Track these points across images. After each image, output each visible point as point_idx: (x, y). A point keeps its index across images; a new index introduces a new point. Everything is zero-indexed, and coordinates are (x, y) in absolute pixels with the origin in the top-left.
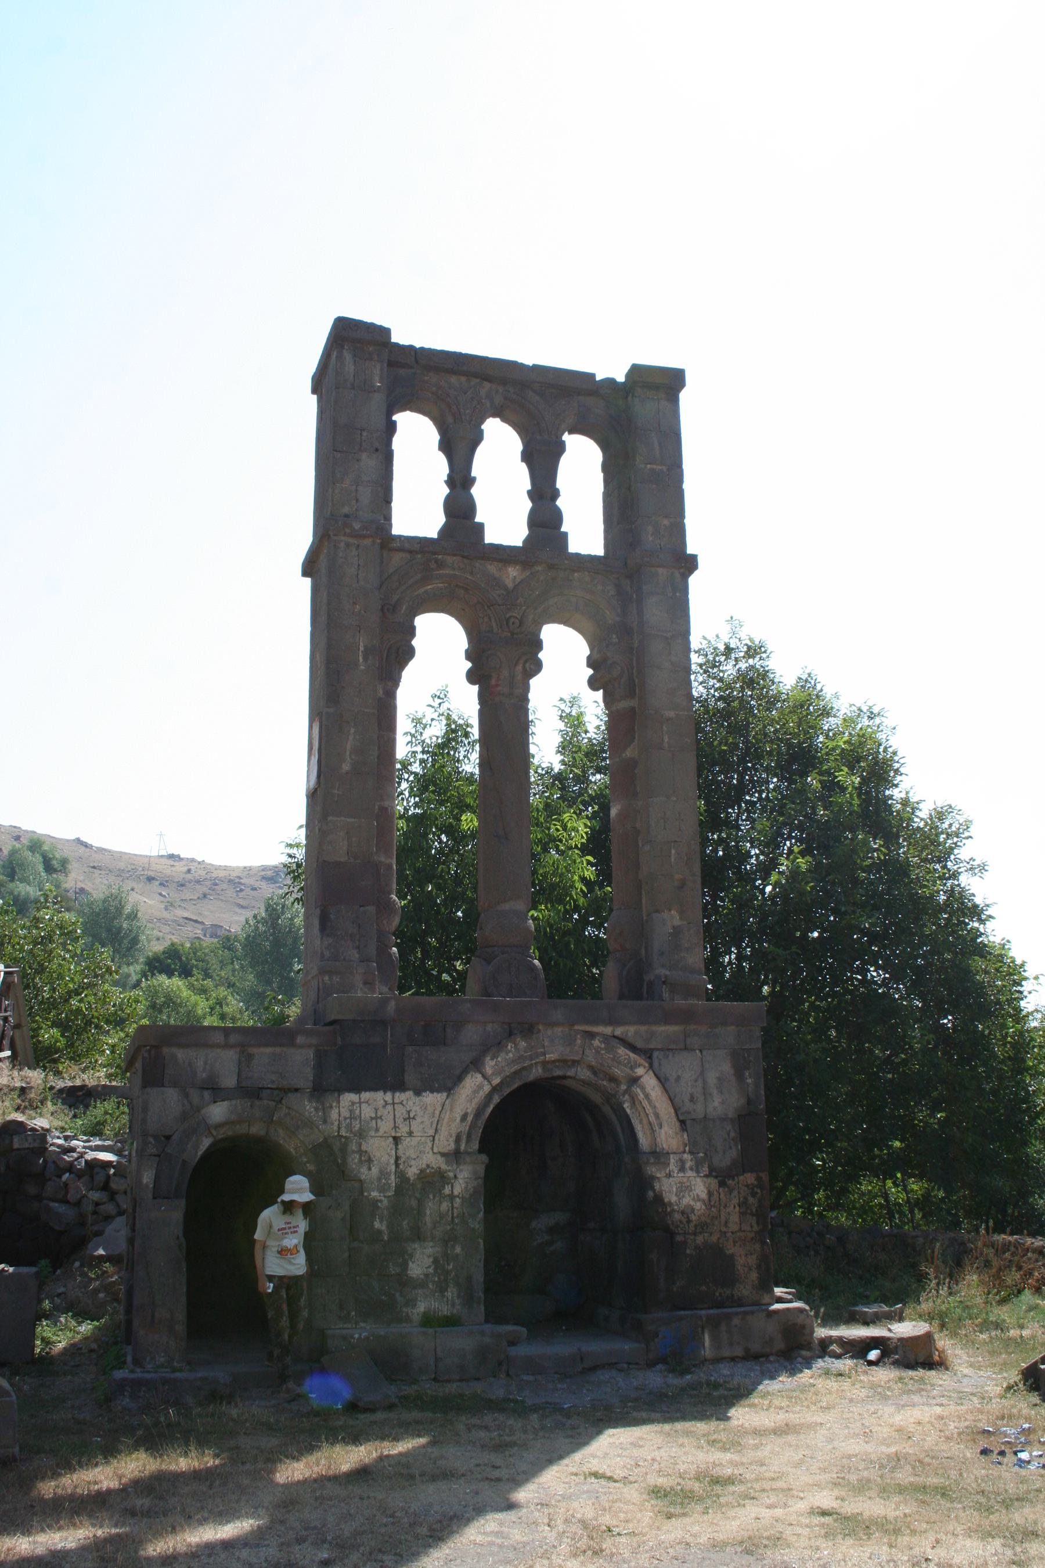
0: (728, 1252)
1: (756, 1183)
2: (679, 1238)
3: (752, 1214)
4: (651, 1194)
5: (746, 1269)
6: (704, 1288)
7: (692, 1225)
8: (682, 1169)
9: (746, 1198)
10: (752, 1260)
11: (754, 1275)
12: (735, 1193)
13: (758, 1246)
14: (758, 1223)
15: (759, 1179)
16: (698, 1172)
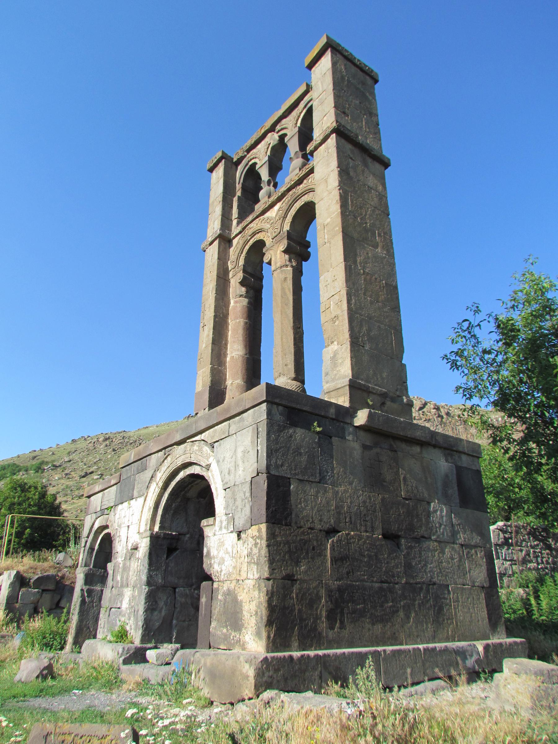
0: (240, 598)
1: (257, 534)
2: (215, 585)
3: (254, 563)
4: (205, 550)
5: (249, 615)
6: (225, 630)
7: (222, 574)
8: (221, 528)
9: (251, 549)
10: (253, 607)
11: (253, 621)
12: (246, 545)
13: (256, 593)
14: (257, 572)
15: (259, 530)
16: (228, 530)
